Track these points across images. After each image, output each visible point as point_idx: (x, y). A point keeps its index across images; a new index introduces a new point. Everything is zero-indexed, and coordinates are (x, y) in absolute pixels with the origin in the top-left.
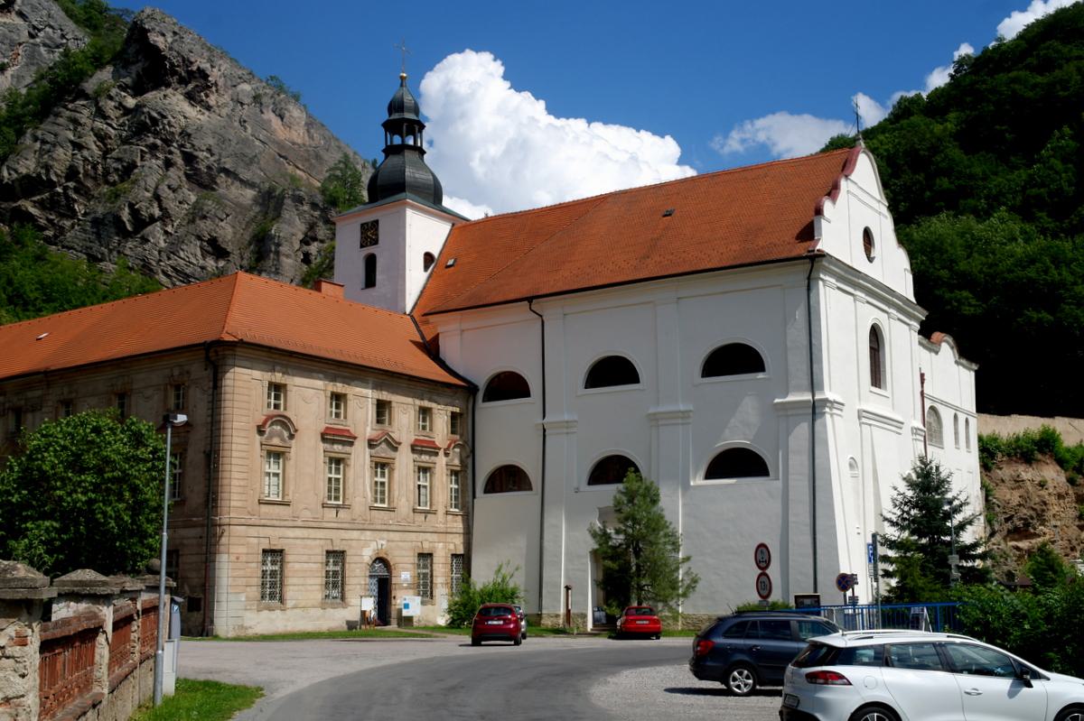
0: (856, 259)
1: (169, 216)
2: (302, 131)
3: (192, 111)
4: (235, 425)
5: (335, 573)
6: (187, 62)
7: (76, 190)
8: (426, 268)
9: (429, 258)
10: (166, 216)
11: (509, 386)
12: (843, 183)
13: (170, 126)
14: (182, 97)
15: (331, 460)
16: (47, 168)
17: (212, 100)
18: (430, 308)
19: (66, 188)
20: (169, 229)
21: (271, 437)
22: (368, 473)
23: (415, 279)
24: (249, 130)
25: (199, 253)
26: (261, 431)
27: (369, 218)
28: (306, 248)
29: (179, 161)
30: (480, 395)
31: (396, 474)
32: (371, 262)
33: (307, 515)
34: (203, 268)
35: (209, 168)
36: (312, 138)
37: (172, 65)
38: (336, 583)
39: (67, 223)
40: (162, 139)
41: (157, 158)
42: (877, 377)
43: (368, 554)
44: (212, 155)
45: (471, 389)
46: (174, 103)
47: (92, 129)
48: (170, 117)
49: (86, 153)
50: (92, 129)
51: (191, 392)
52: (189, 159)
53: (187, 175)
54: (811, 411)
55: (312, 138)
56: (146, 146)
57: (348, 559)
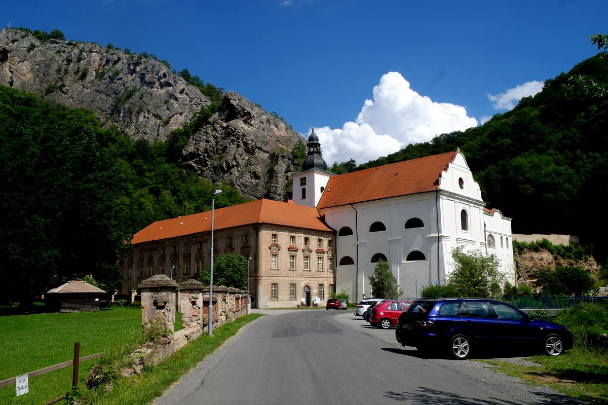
0: (456, 190)
1: (239, 165)
3: (246, 127)
4: (263, 247)
5: (293, 290)
6: (244, 109)
7: (208, 157)
8: (321, 192)
9: (322, 189)
10: (238, 165)
11: (346, 231)
12: (450, 165)
13: (239, 133)
15: (291, 256)
16: (198, 149)
17: (253, 122)
18: (323, 206)
19: (204, 156)
20: (239, 169)
21: (273, 250)
22: (302, 260)
23: (318, 195)
24: (266, 133)
25: (250, 177)
26: (270, 249)
27: (303, 176)
28: (286, 174)
29: (242, 145)
30: (338, 234)
31: (311, 260)
32: (304, 191)
33: (284, 273)
34: (251, 183)
35: (252, 147)
36: (288, 133)
37: (238, 111)
38: (293, 294)
39: (205, 168)
41: (235, 144)
42: (464, 226)
43: (303, 285)
44: (253, 142)
45: (334, 232)
46: (239, 124)
47: (212, 135)
49: (210, 143)
50: (212, 135)
51: (250, 237)
52: (245, 144)
53: (245, 150)
54: (438, 239)
55: (288, 133)
56: (231, 140)
57: (297, 286)
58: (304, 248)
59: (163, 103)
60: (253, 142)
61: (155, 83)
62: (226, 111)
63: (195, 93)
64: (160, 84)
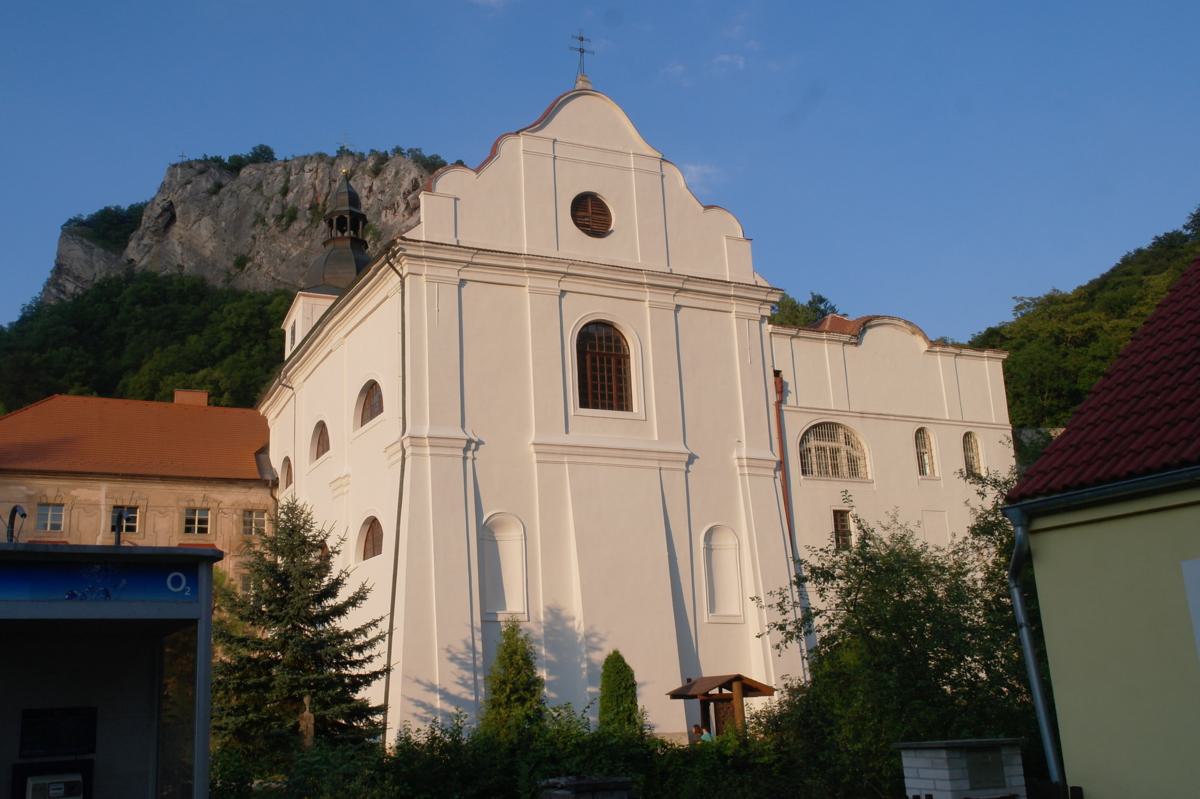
64: (408, 204)
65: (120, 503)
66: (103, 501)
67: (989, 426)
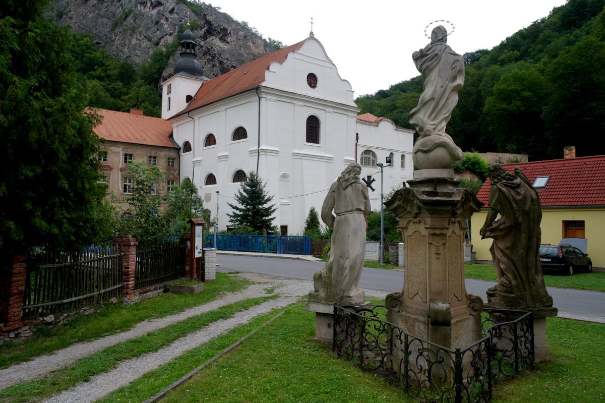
2: (262, 48)
3: (222, 45)
13: (214, 51)
14: (218, 39)
17: (229, 40)
27: (168, 84)
29: (218, 65)
32: (169, 99)
36: (266, 51)
40: (211, 57)
41: (210, 64)
48: (214, 48)
53: (220, 70)
55: (266, 51)
56: (207, 60)
58: (124, 166)
59: (154, 24)
60: (229, 61)
61: (147, 3)
62: (203, 28)
63: (184, 12)
65: (127, 153)
66: (121, 152)
67: (408, 153)
